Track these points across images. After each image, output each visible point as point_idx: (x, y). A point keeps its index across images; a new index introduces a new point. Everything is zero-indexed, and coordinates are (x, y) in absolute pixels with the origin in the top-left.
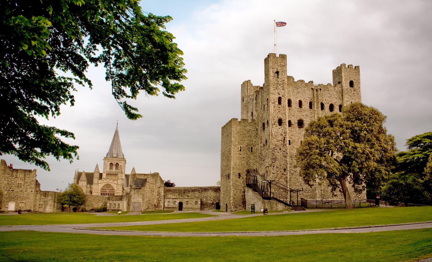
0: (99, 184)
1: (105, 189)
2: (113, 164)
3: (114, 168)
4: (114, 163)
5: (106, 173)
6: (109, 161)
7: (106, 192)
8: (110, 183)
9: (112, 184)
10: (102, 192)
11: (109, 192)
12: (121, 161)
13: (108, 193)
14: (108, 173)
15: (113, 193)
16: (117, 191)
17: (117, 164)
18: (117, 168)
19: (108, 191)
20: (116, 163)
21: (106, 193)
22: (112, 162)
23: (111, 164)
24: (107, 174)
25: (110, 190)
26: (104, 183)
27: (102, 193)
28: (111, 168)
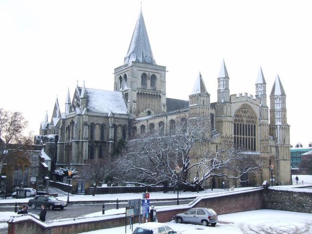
2: (148, 75)
3: (149, 82)
5: (137, 91)
7: (242, 121)
8: (249, 104)
9: (252, 105)
10: (236, 120)
11: (247, 121)
12: (160, 72)
13: (245, 124)
15: (253, 125)
16: (262, 120)
17: (154, 77)
18: (153, 84)
19: (245, 119)
20: (151, 74)
22: (145, 72)
24: (138, 93)
25: (249, 117)
27: (236, 123)
28: (144, 83)
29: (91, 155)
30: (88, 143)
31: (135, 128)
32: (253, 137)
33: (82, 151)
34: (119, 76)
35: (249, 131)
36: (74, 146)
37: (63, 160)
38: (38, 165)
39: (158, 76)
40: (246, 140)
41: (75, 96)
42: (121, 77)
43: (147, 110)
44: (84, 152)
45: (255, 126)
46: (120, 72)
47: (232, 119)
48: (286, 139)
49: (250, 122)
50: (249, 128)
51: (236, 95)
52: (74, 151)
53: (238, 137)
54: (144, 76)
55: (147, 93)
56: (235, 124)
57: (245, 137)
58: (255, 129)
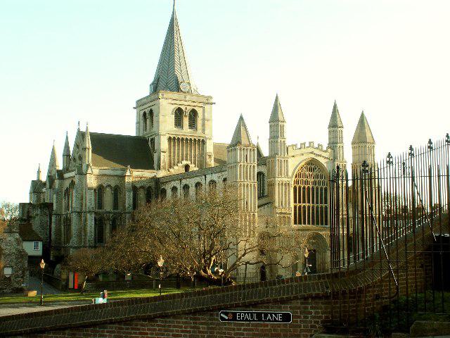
1: (305, 176)
3: (186, 121)
5: (168, 136)
6: (175, 102)
7: (307, 183)
10: (297, 182)
11: (315, 183)
12: (200, 105)
14: (172, 136)
17: (194, 114)
18: (193, 124)
20: (189, 108)
24: (170, 138)
25: (317, 176)
26: (303, 154)
28: (178, 123)
29: (99, 237)
30: (93, 216)
31: (164, 191)
33: (85, 225)
34: (142, 112)
35: (300, 195)
36: (74, 217)
37: (60, 239)
38: (14, 251)
39: (199, 111)
40: (313, 210)
41: (77, 146)
42: (145, 114)
43: (185, 162)
44: (88, 229)
46: (144, 107)
49: (319, 183)
51: (296, 145)
52: (74, 228)
54: (179, 113)
56: (295, 188)
57: (315, 205)
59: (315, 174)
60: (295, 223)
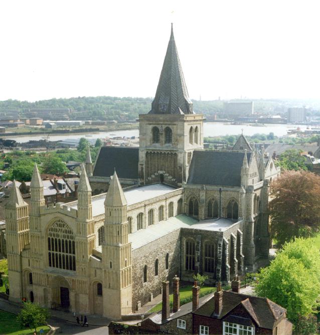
0: (40, 216)
1: (56, 230)
3: (162, 138)
4: (162, 128)
6: (151, 123)
7: (58, 236)
9: (67, 220)
11: (64, 237)
17: (168, 131)
18: (169, 139)
20: (164, 127)
21: (58, 239)
22: (157, 126)
23: (155, 131)
24: (147, 152)
25: (66, 232)
27: (51, 238)
28: (156, 139)
32: (72, 255)
43: (161, 172)
45: (74, 242)
47: (44, 234)
48: (112, 265)
49: (68, 237)
50: (67, 244)
53: (53, 254)
55: (158, 153)
56: (49, 239)
58: (74, 246)
59: (63, 229)
60: (50, 266)
